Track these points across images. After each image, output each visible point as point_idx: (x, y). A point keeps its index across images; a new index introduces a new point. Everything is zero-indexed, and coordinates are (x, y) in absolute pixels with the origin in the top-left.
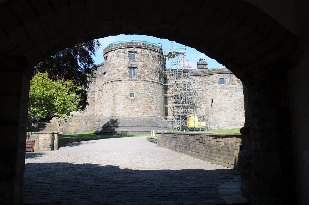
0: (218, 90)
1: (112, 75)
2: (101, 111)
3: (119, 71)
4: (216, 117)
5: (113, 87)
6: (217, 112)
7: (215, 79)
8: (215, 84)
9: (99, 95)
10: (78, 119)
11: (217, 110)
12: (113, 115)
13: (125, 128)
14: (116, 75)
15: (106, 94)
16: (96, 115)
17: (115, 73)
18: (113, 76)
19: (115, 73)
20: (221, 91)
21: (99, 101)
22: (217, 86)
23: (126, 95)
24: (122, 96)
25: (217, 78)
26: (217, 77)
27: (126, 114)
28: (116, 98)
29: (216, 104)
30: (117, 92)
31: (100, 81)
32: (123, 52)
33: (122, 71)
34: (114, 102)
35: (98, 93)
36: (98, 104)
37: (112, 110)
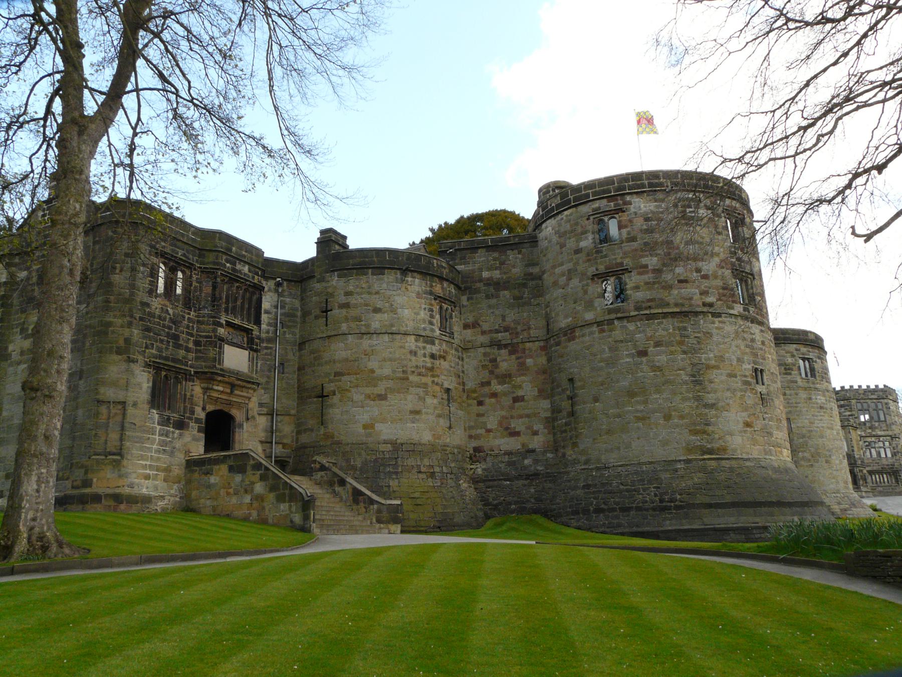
0: (803, 395)
1: (671, 287)
2: (515, 434)
3: (705, 277)
4: (807, 477)
5: (688, 337)
6: (809, 460)
7: (790, 360)
8: (790, 374)
9: (497, 367)
10: (426, 462)
11: (807, 455)
12: (704, 453)
13: (787, 510)
14: (691, 291)
15: (644, 359)
16: (477, 450)
17: (686, 281)
18: (675, 292)
19: (686, 281)
20: (810, 399)
21: (497, 387)
22: (796, 382)
23: (745, 376)
24: (730, 375)
25: (793, 356)
26: (795, 353)
27: (755, 452)
28: (706, 383)
29: (804, 436)
30: (708, 356)
31: (490, 307)
32: (708, 208)
33: (716, 277)
34: (698, 399)
35: (485, 354)
36: (487, 401)
37: (695, 432)
